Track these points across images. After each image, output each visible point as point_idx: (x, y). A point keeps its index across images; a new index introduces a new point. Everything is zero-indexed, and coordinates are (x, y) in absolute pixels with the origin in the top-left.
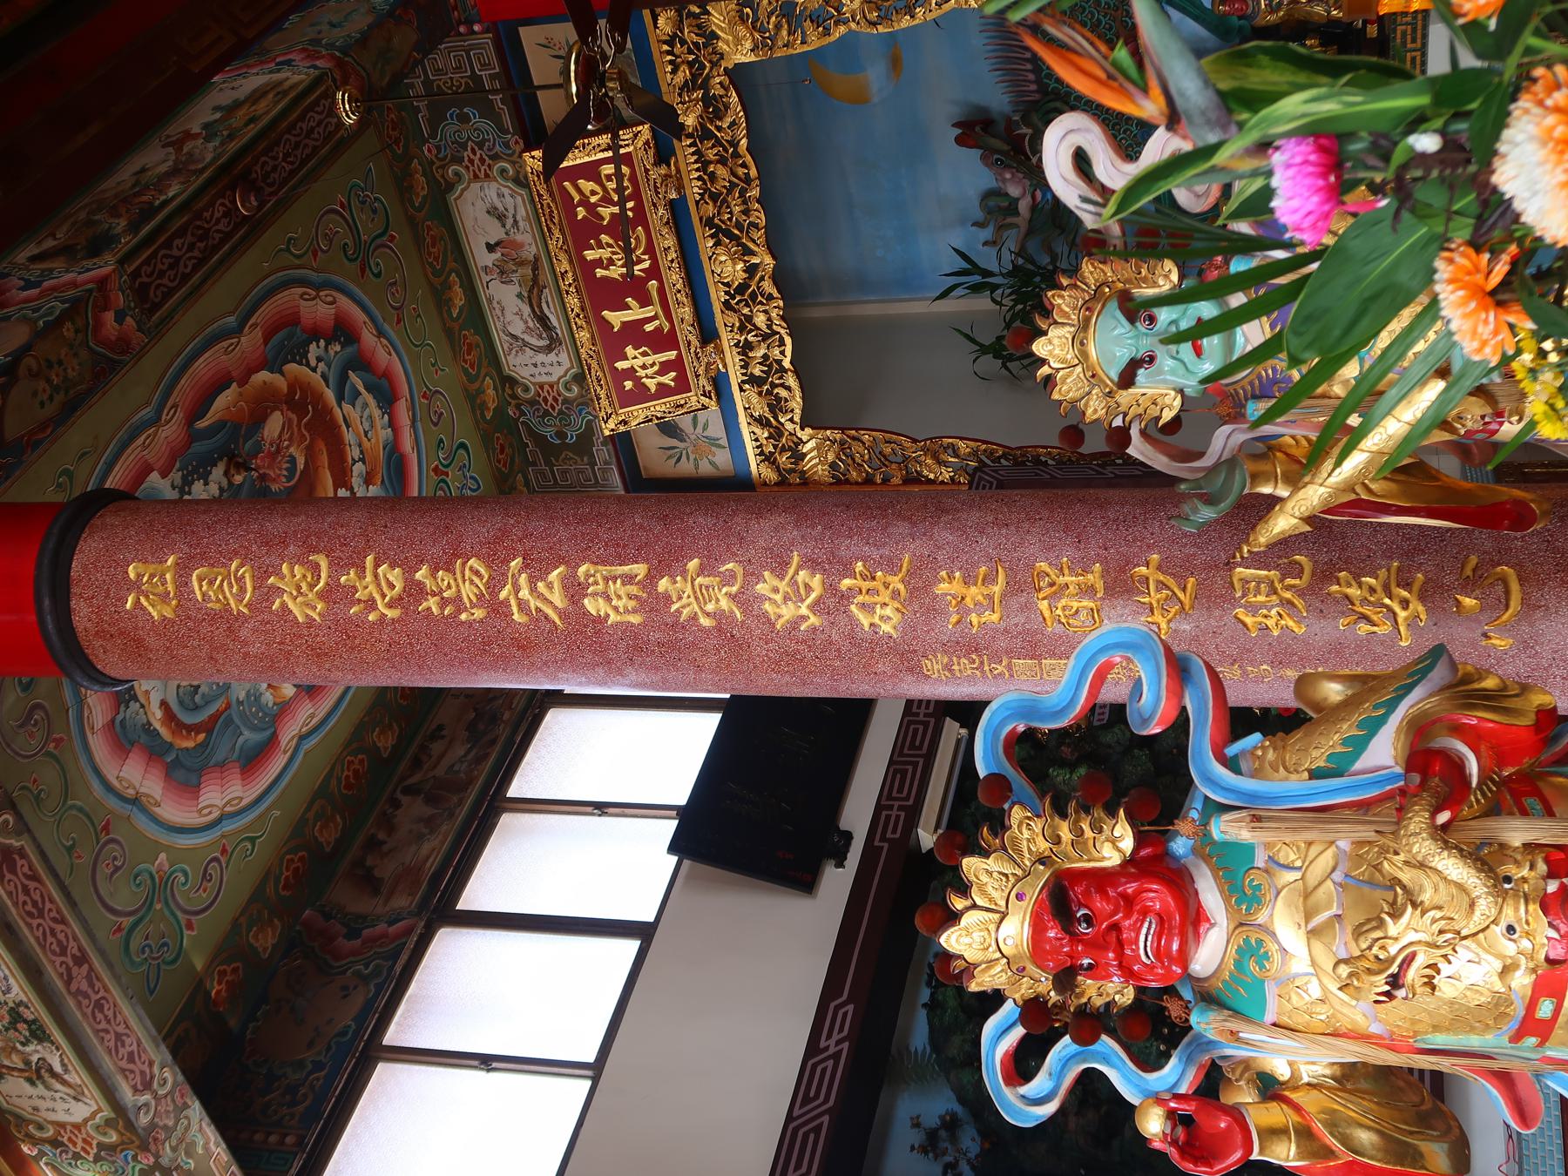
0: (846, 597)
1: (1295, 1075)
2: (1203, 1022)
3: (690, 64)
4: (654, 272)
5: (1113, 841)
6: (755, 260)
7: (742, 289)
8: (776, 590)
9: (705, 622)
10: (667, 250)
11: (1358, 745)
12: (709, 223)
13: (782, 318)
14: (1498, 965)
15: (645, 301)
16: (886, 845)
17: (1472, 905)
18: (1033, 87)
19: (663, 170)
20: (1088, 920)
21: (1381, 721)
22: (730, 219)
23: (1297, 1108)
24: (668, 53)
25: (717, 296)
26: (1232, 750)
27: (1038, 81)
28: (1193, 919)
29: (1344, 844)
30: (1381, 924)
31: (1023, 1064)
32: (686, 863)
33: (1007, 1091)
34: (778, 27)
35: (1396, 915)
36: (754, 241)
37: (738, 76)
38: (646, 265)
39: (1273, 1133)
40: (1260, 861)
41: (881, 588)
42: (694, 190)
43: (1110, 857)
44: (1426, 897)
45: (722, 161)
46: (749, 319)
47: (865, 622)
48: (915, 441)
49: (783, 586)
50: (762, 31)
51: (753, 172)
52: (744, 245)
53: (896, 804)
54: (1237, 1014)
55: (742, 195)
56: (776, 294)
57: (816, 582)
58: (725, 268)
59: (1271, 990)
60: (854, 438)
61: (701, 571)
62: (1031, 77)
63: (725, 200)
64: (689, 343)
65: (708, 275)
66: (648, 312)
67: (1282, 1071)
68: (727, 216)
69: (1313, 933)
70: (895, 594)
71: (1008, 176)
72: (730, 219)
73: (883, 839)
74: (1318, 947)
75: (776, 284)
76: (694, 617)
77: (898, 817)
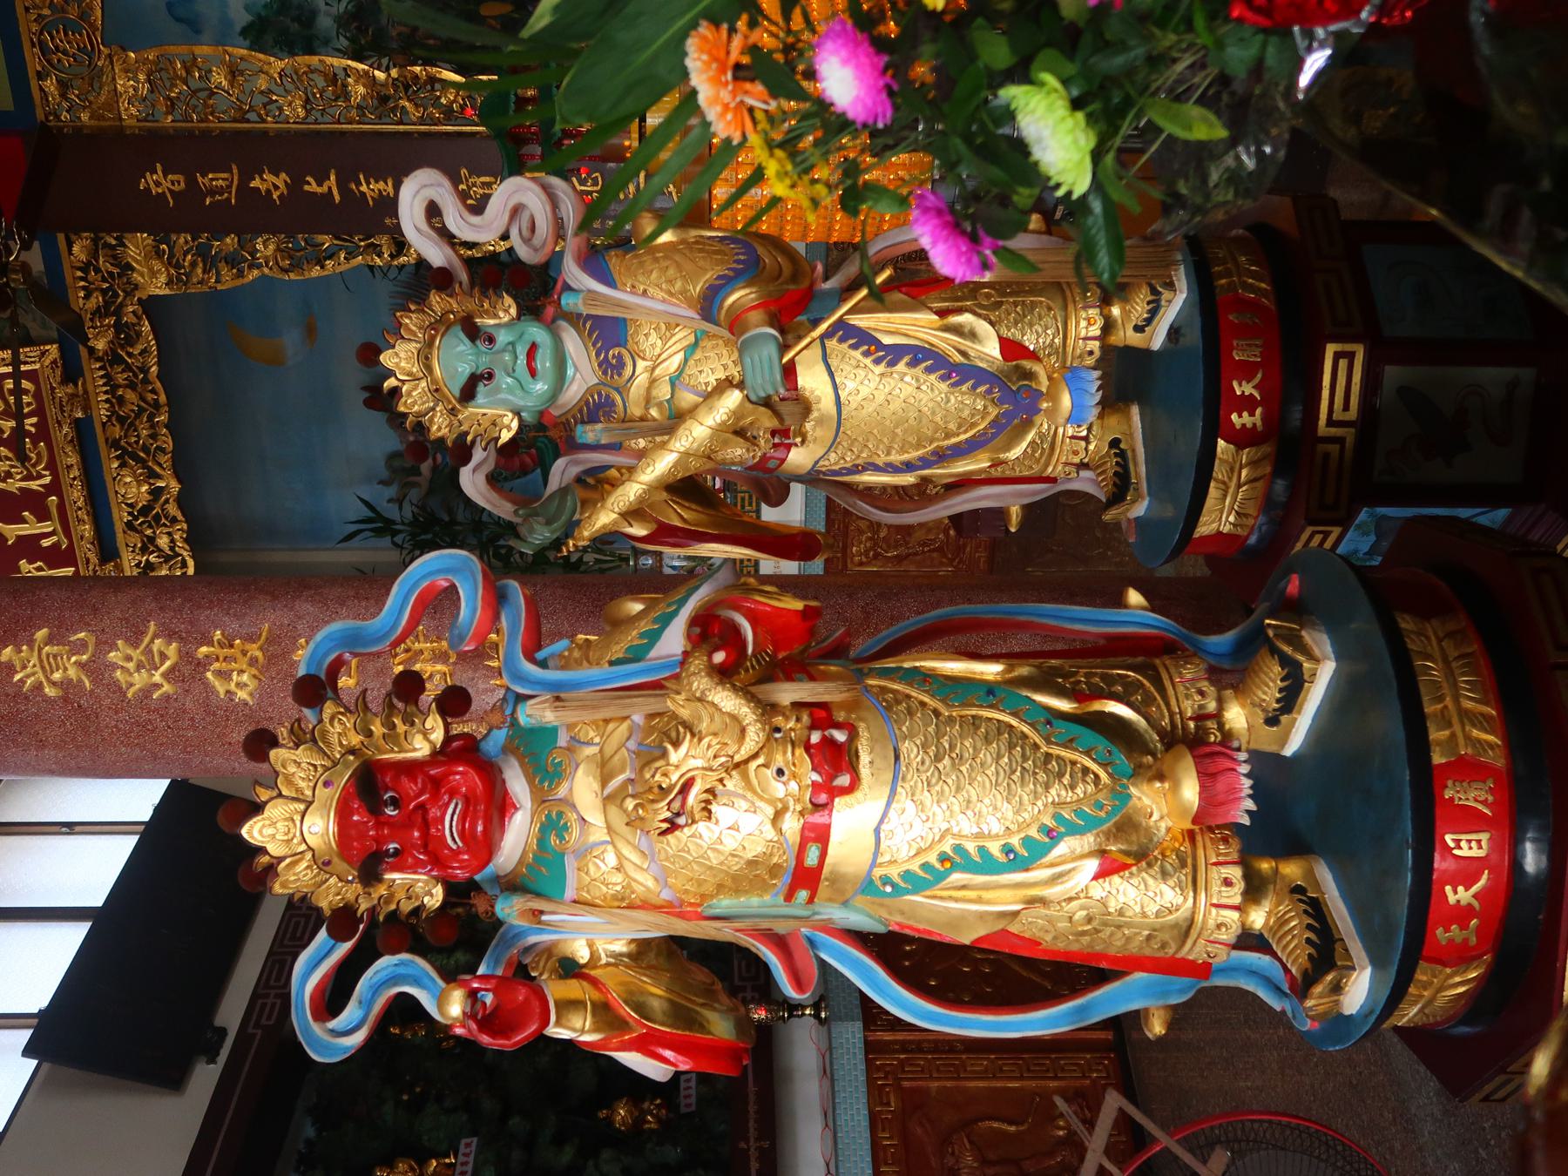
0: (203, 665)
1: (594, 956)
2: (509, 909)
3: (104, 292)
4: (55, 488)
5: (425, 734)
6: (162, 484)
7: (145, 511)
8: (129, 658)
9: (50, 691)
10: (69, 467)
11: (654, 637)
12: (115, 444)
13: (186, 540)
14: (770, 811)
15: (43, 516)
16: (259, 1032)
17: (743, 731)
19: (70, 389)
20: (394, 802)
21: (675, 613)
22: (137, 442)
23: (594, 982)
24: (82, 279)
25: (121, 516)
26: (540, 655)
28: (501, 806)
29: (638, 718)
30: (664, 754)
31: (333, 998)
32: (46, 1066)
33: (316, 1027)
34: (193, 265)
35: (676, 744)
36: (160, 465)
37: (152, 306)
38: (47, 480)
39: (567, 1006)
40: (563, 740)
41: (239, 655)
42: (103, 412)
43: (420, 748)
44: (704, 726)
45: (131, 386)
46: (152, 540)
47: (220, 687)
49: (136, 654)
50: (178, 266)
51: (163, 398)
52: (149, 468)
53: (273, 992)
54: (538, 895)
55: (151, 417)
56: (180, 517)
57: (172, 650)
58: (130, 489)
59: (570, 863)
61: (50, 640)
63: (132, 424)
64: (88, 561)
65: (111, 495)
66: (46, 527)
67: (582, 955)
68: (133, 439)
69: (607, 800)
70: (253, 662)
72: (137, 442)
73: (257, 1025)
74: (613, 811)
75: (180, 507)
76: (38, 687)
77: (274, 1005)
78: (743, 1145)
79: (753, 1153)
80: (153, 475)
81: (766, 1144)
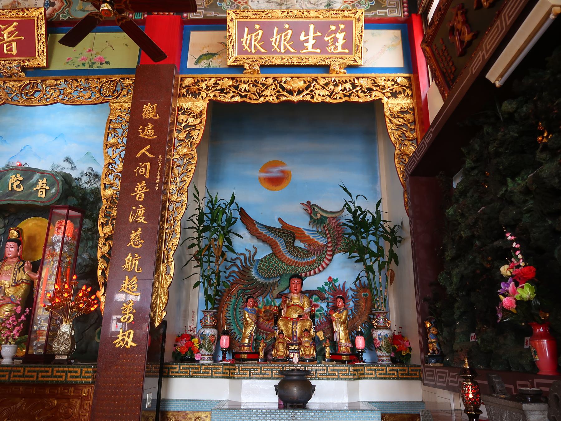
63: (324, 88)
80: (299, 92)
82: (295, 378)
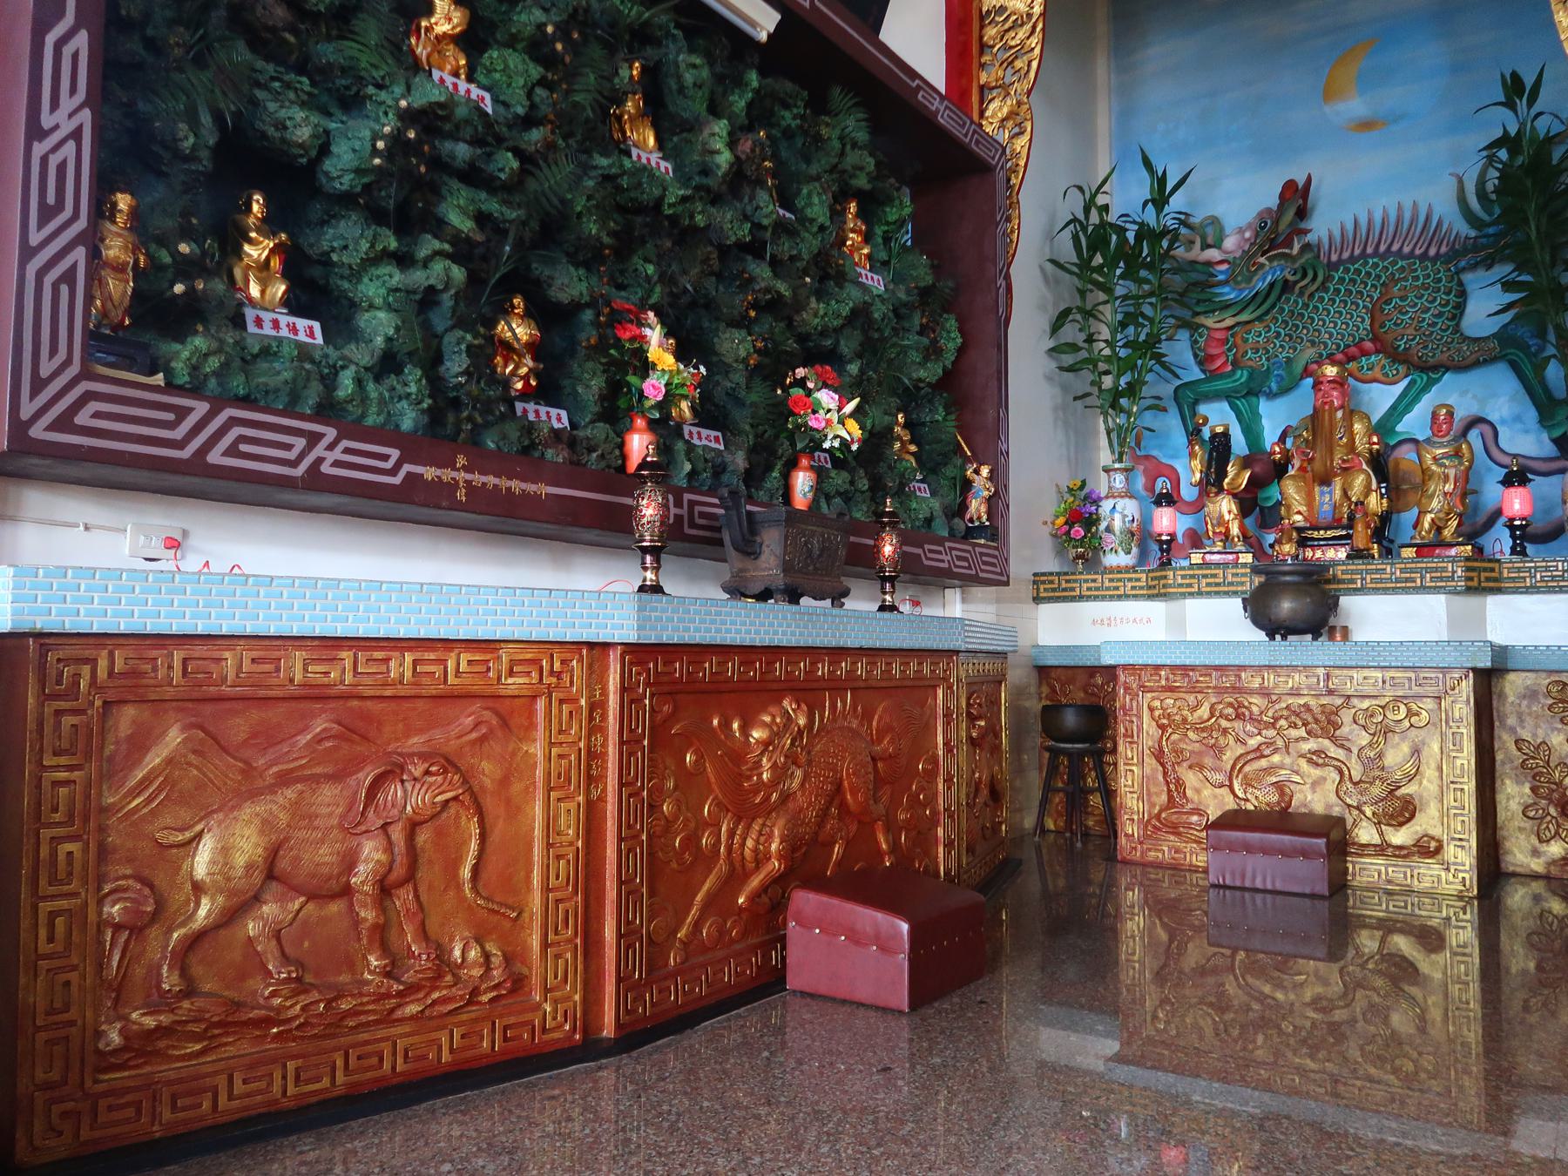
18: (1334, 258)
27: (1340, 262)
48: (1029, 92)
60: (1034, 27)
62: (1346, 255)
71: (1247, 235)
78: (461, 461)
79: (447, 475)
81: (461, 495)
82: (1288, 578)
